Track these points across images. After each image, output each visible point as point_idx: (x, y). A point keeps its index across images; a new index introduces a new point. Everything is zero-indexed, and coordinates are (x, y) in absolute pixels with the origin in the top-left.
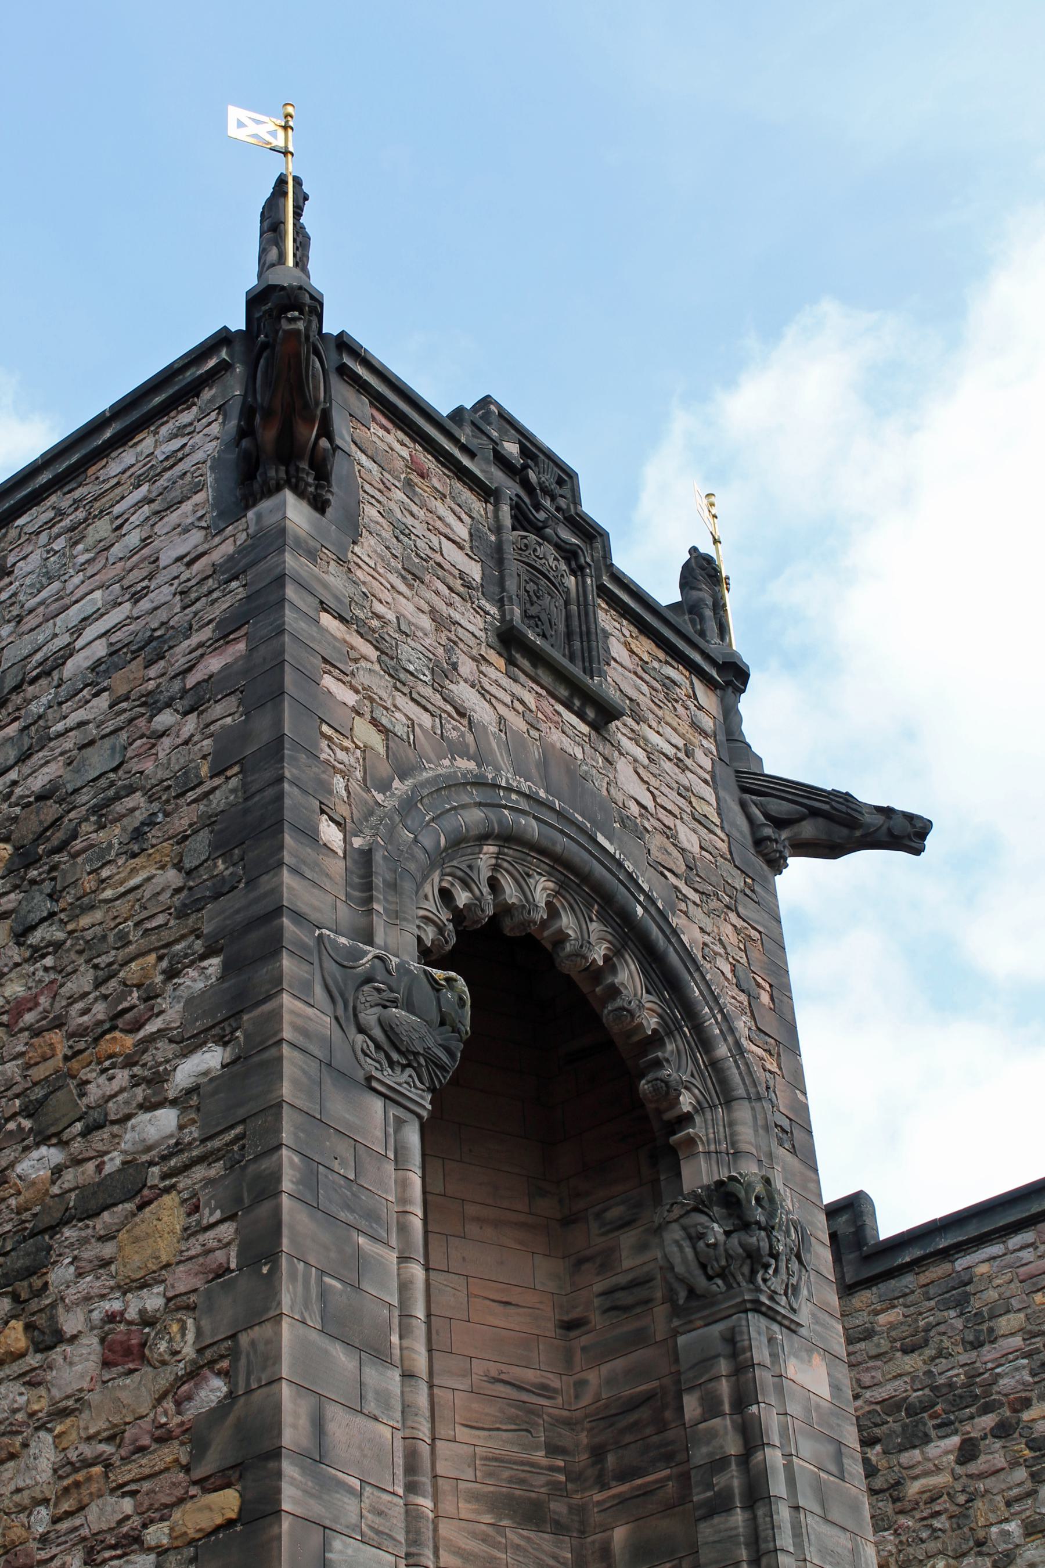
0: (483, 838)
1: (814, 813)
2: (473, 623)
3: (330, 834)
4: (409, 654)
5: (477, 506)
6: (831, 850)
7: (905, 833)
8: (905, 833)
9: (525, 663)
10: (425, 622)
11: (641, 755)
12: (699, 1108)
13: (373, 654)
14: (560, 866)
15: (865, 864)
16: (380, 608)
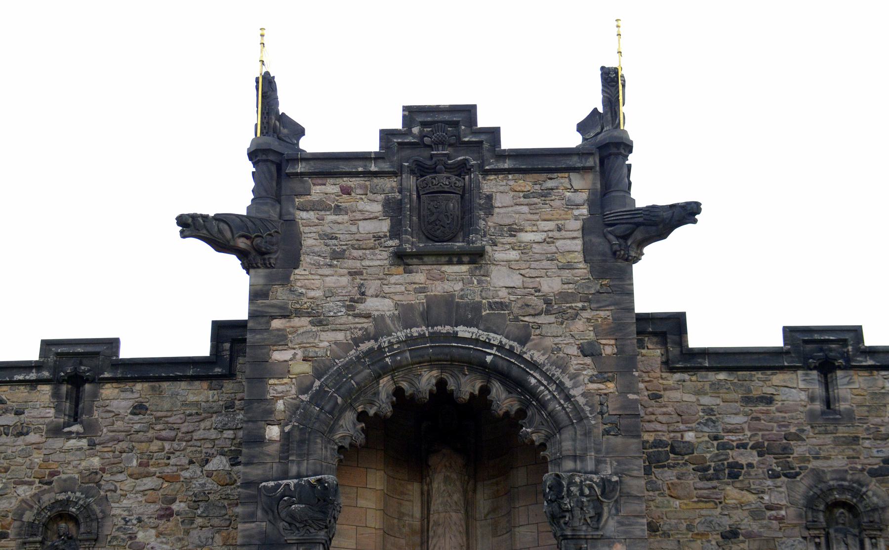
0: (379, 377)
1: (638, 225)
2: (381, 258)
3: (273, 432)
4: (332, 306)
5: (390, 183)
6: (662, 235)
7: (687, 213)
8: (687, 213)
9: (415, 261)
10: (345, 280)
11: (513, 255)
12: (548, 437)
13: (305, 321)
14: (432, 363)
15: (681, 233)
16: (312, 294)
